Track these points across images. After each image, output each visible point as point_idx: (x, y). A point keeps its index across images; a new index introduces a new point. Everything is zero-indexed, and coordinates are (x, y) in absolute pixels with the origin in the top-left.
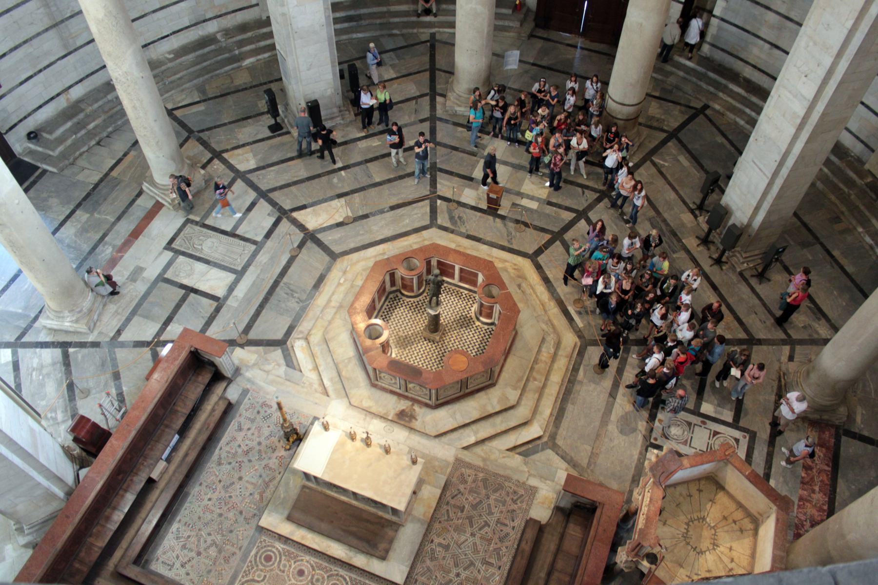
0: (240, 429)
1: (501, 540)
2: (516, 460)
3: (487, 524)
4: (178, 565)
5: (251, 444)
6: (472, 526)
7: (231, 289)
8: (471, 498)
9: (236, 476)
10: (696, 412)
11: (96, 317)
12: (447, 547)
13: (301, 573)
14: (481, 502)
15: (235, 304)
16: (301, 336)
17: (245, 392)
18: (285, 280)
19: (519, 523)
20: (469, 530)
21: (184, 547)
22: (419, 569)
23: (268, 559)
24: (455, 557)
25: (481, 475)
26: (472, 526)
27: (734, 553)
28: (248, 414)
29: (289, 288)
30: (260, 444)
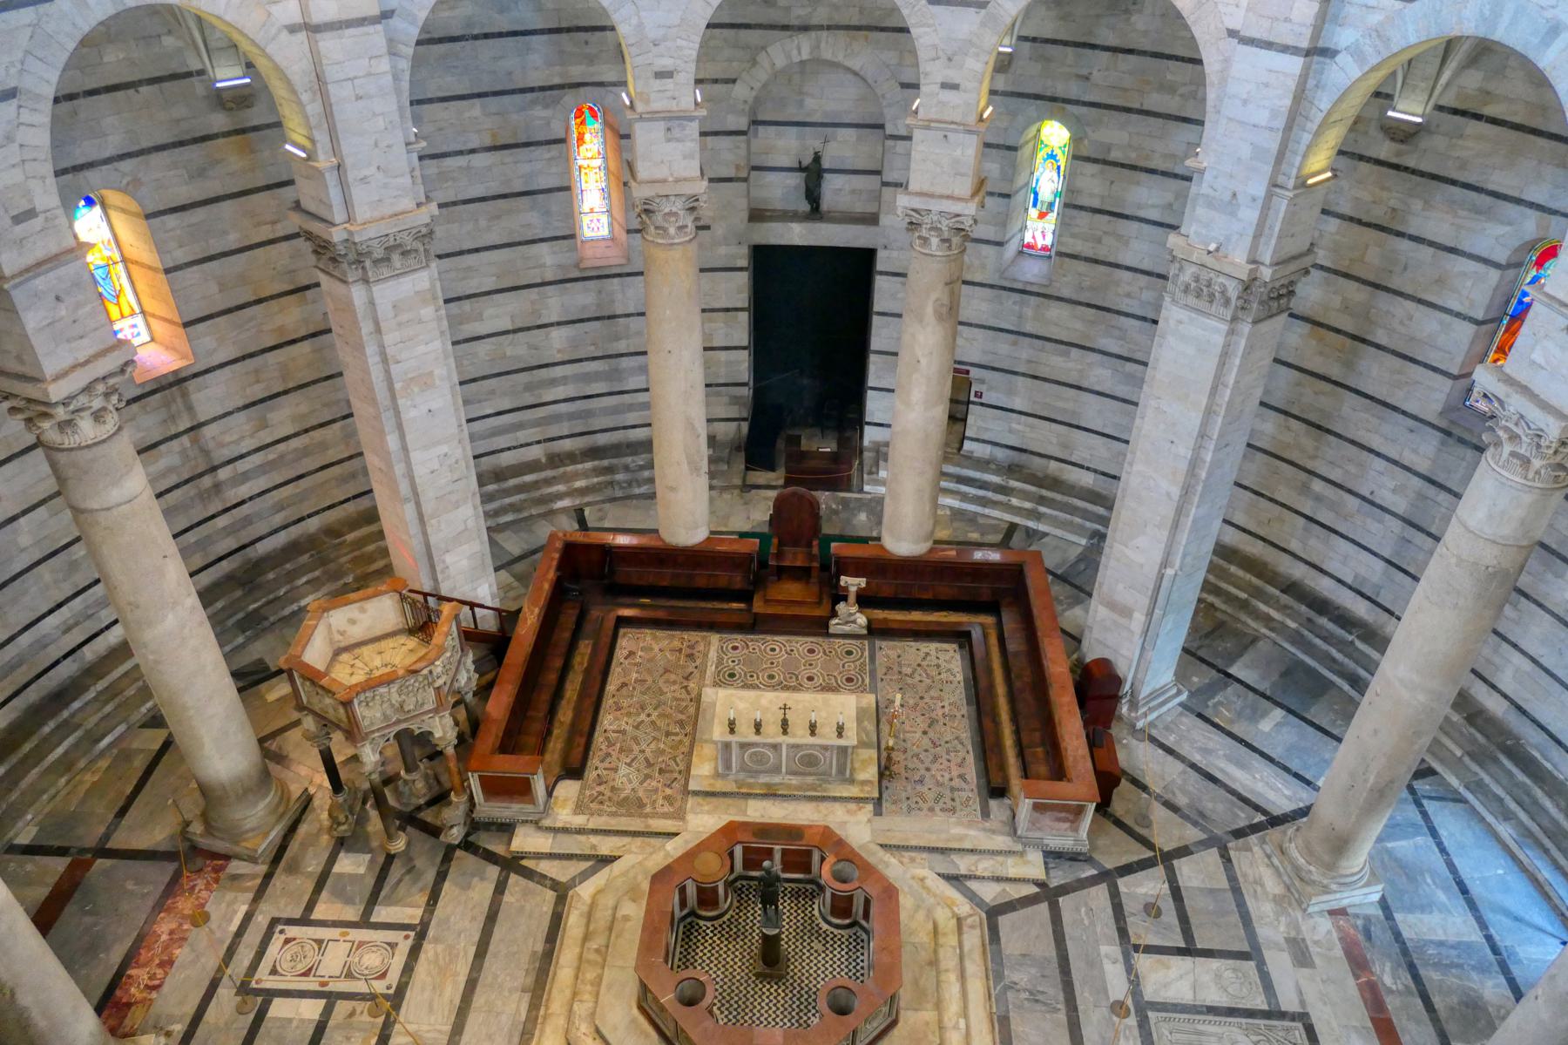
0: (961, 776)
1: (608, 755)
2: (605, 846)
3: (629, 765)
4: (933, 653)
5: (937, 765)
6: (647, 760)
7: (1129, 968)
8: (654, 784)
9: (931, 734)
10: (331, 998)
11: (1276, 861)
12: (668, 734)
13: (810, 679)
14: (641, 783)
15: (1104, 949)
16: (969, 921)
17: (986, 814)
18: (1062, 1016)
19: (590, 774)
20: (648, 754)
21: (938, 666)
22: (692, 710)
23: (849, 680)
24: (657, 729)
25: (648, 809)
26: (647, 760)
27: (348, 670)
28: (964, 795)
29: (1045, 1004)
30: (928, 769)
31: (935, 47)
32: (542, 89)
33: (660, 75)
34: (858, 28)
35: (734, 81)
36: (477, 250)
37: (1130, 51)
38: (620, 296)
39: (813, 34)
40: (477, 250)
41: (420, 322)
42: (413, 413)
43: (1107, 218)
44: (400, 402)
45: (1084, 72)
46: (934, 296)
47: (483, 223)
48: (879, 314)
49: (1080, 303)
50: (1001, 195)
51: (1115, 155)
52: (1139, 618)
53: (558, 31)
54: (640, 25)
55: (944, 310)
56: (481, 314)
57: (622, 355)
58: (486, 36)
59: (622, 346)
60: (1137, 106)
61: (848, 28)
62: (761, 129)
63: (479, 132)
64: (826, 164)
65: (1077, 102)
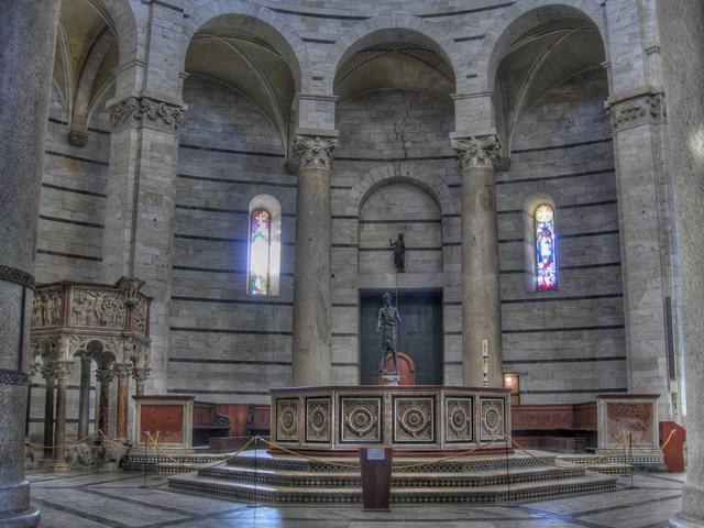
31: (461, 60)
32: (239, 182)
33: (315, 78)
34: (422, 159)
35: (350, 188)
36: (184, 268)
37: (573, 146)
38: (270, 318)
39: (397, 163)
40: (184, 268)
41: (163, 162)
42: (144, 216)
43: (584, 238)
44: (140, 204)
45: (551, 162)
46: (479, 193)
47: (191, 252)
48: (448, 333)
49: (581, 298)
50: (518, 240)
51: (580, 200)
52: (662, 361)
53: (253, 154)
54: (307, 54)
55: (487, 203)
56: (178, 312)
57: (268, 363)
58: (213, 150)
59: (269, 356)
60: (584, 171)
61: (415, 159)
62: (366, 225)
63: (199, 198)
64: (407, 245)
65: (551, 178)
